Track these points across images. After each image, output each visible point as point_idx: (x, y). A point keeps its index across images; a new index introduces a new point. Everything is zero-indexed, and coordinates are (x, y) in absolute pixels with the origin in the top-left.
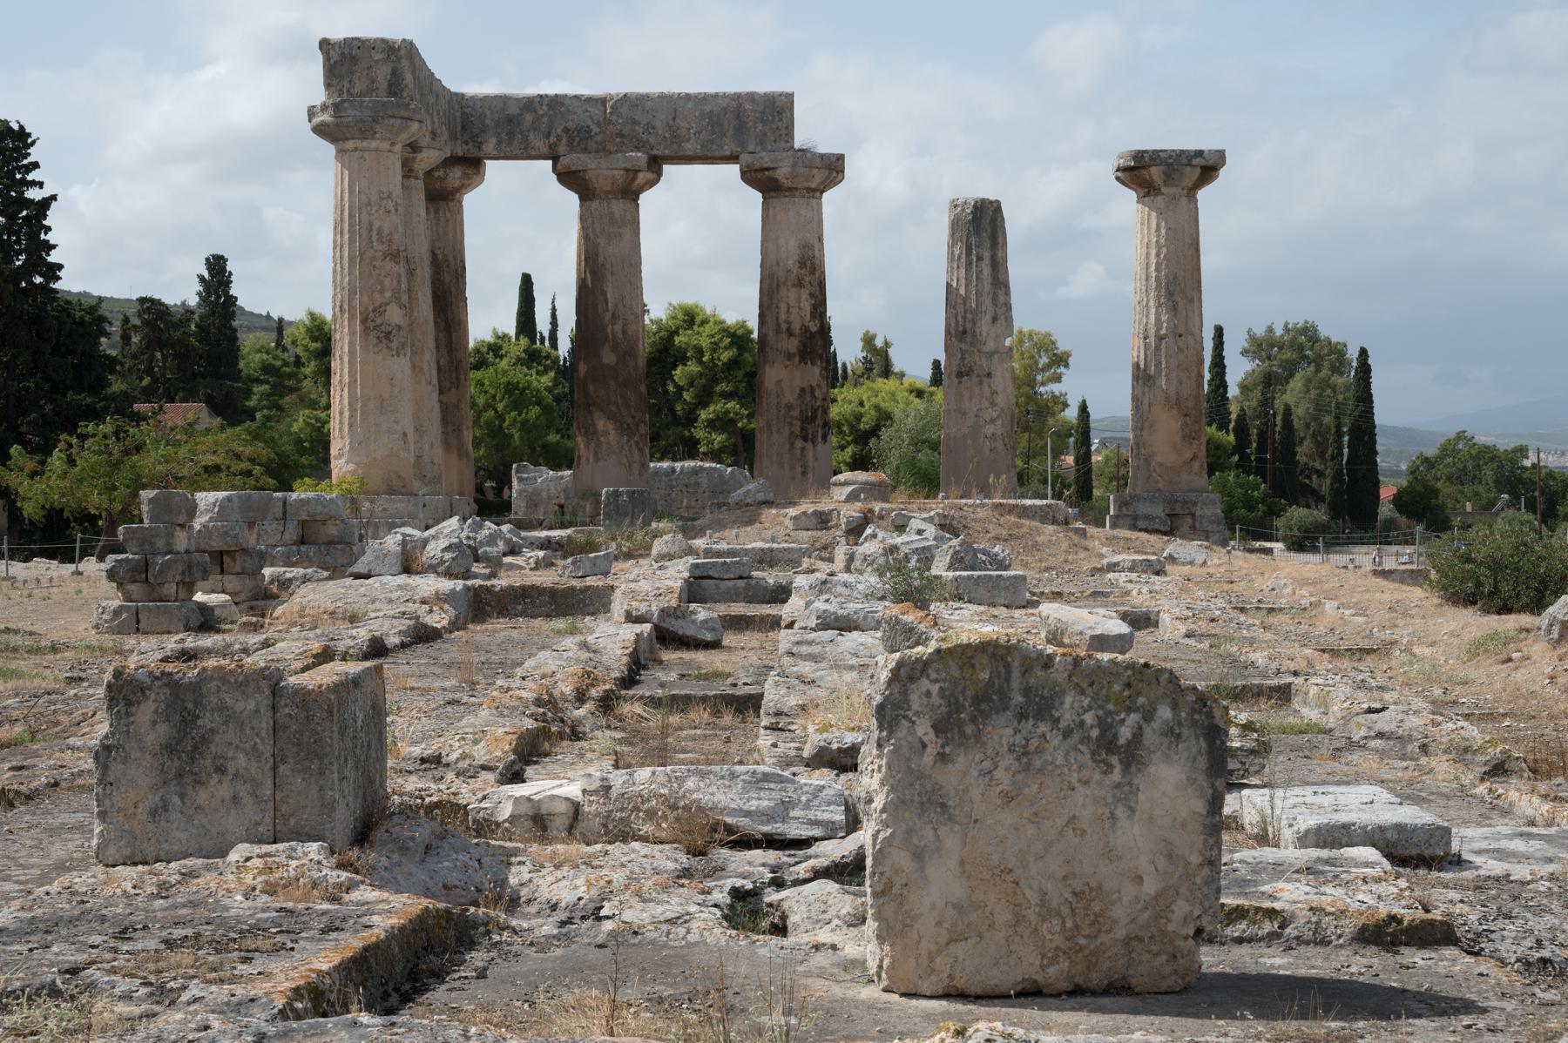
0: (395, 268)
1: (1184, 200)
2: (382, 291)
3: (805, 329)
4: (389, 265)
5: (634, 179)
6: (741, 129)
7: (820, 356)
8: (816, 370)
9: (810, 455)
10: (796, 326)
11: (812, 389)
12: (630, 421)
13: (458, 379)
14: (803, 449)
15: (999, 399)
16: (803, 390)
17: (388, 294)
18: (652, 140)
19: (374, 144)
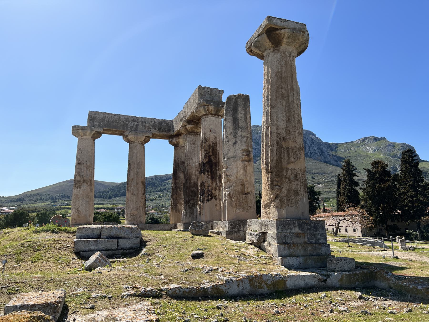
0: (80, 167)
5: (186, 129)
7: (208, 171)
8: (206, 176)
11: (203, 182)
12: (187, 199)
13: (177, 191)
15: (233, 178)
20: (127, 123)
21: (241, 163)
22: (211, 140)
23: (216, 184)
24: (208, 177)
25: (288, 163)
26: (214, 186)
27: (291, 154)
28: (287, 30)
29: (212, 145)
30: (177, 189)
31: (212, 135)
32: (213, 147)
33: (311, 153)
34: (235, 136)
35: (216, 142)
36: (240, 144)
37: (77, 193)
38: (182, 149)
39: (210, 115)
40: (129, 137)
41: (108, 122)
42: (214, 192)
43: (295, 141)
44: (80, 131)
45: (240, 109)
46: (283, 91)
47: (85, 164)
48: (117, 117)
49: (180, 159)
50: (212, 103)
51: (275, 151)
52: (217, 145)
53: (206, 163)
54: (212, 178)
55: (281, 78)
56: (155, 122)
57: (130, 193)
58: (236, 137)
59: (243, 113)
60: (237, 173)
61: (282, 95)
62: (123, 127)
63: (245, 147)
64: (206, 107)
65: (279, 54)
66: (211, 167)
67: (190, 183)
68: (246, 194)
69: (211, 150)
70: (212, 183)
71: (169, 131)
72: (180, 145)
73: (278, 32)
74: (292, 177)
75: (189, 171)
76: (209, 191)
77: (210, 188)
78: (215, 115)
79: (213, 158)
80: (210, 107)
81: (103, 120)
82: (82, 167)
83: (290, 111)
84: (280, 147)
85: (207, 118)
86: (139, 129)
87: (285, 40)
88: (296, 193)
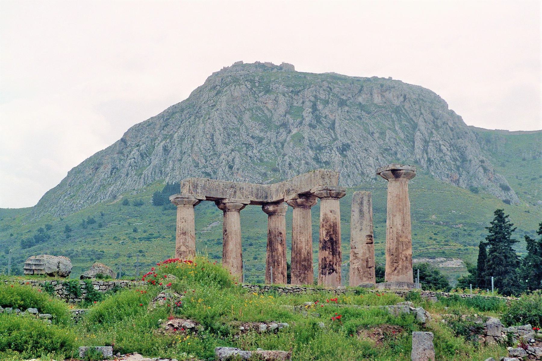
1: (394, 182)
7: (329, 248)
8: (327, 252)
9: (324, 278)
10: (322, 240)
15: (360, 256)
18: (298, 189)
22: (332, 221)
23: (337, 259)
24: (329, 253)
25: (403, 251)
26: (335, 260)
33: (429, 160)
34: (361, 224)
42: (334, 266)
43: (406, 237)
45: (365, 203)
47: (189, 234)
51: (395, 243)
54: (333, 254)
62: (223, 194)
63: (369, 234)
66: (332, 244)
67: (300, 257)
69: (332, 230)
71: (266, 197)
73: (399, 171)
74: (404, 259)
75: (299, 246)
76: (330, 265)
77: (331, 263)
79: (334, 236)
82: (187, 237)
84: (398, 240)
85: (328, 201)
87: (402, 175)
88: (406, 268)
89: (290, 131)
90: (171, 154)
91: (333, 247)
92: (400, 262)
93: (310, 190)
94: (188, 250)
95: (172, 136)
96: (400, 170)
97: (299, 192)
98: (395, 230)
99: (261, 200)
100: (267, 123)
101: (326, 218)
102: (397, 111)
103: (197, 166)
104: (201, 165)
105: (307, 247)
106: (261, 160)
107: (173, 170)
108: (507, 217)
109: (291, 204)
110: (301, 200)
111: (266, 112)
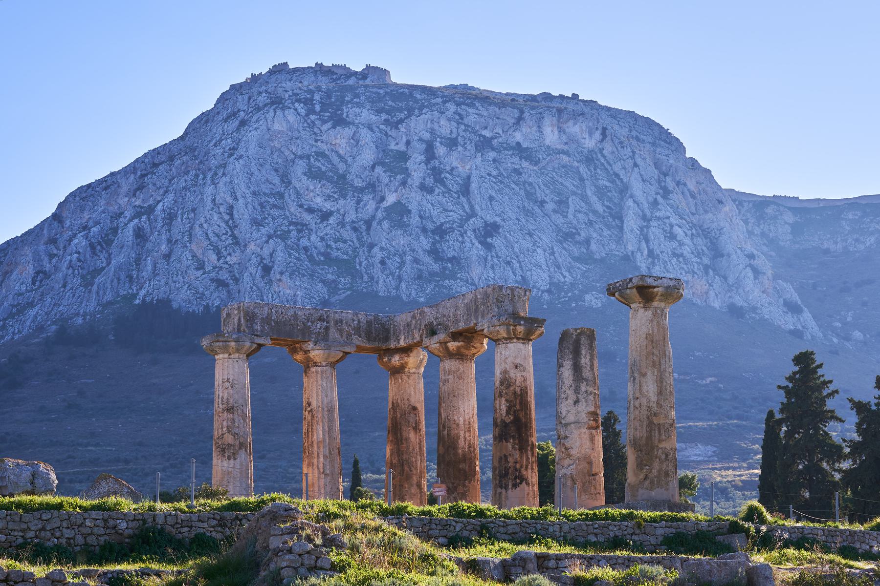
1: (641, 311)
2: (222, 428)
3: (503, 421)
4: (225, 414)
5: (447, 348)
6: (476, 311)
7: (514, 437)
8: (510, 446)
10: (499, 420)
11: (505, 456)
13: (403, 470)
14: (500, 493)
16: (501, 458)
17: (225, 429)
19: (221, 356)
20: (310, 324)
21: (587, 431)
22: (518, 383)
23: (528, 459)
24: (513, 447)
25: (660, 441)
27: (662, 432)
28: (660, 289)
29: (519, 393)
30: (402, 465)
31: (519, 375)
32: (521, 394)
33: (651, 253)
34: (577, 391)
35: (526, 387)
36: (585, 404)
37: (230, 469)
38: (411, 378)
39: (515, 340)
40: (313, 354)
41: (276, 323)
42: (524, 472)
44: (233, 344)
46: (655, 358)
48: (291, 313)
49: (408, 400)
50: (522, 322)
52: (527, 393)
53: (511, 422)
55: (652, 341)
56: (359, 321)
57: (316, 471)
58: (579, 393)
59: (588, 357)
60: (581, 446)
61: (653, 362)
62: (303, 334)
63: (592, 409)
64: (512, 327)
65: (650, 312)
67: (456, 454)
68: (593, 475)
70: (521, 457)
71: (387, 339)
72: (407, 370)
74: (663, 457)
76: (516, 470)
77: (518, 466)
78: (523, 339)
79: (521, 415)
80: (518, 327)
81: (267, 320)
83: (662, 382)
84: (650, 423)
85: (510, 345)
86: (331, 337)
87: (657, 298)
89: (383, 199)
90: (149, 245)
91: (520, 435)
92: (656, 465)
93: (476, 325)
94: (237, 443)
95: (151, 210)
96: (654, 287)
97: (453, 330)
98: (644, 401)
99: (377, 345)
100: (341, 184)
101: (506, 379)
102: (589, 159)
103: (201, 266)
104: (208, 268)
105: (467, 434)
106: (326, 255)
107: (155, 274)
108: (820, 366)
109: (436, 352)
110: (457, 344)
111: (335, 160)
